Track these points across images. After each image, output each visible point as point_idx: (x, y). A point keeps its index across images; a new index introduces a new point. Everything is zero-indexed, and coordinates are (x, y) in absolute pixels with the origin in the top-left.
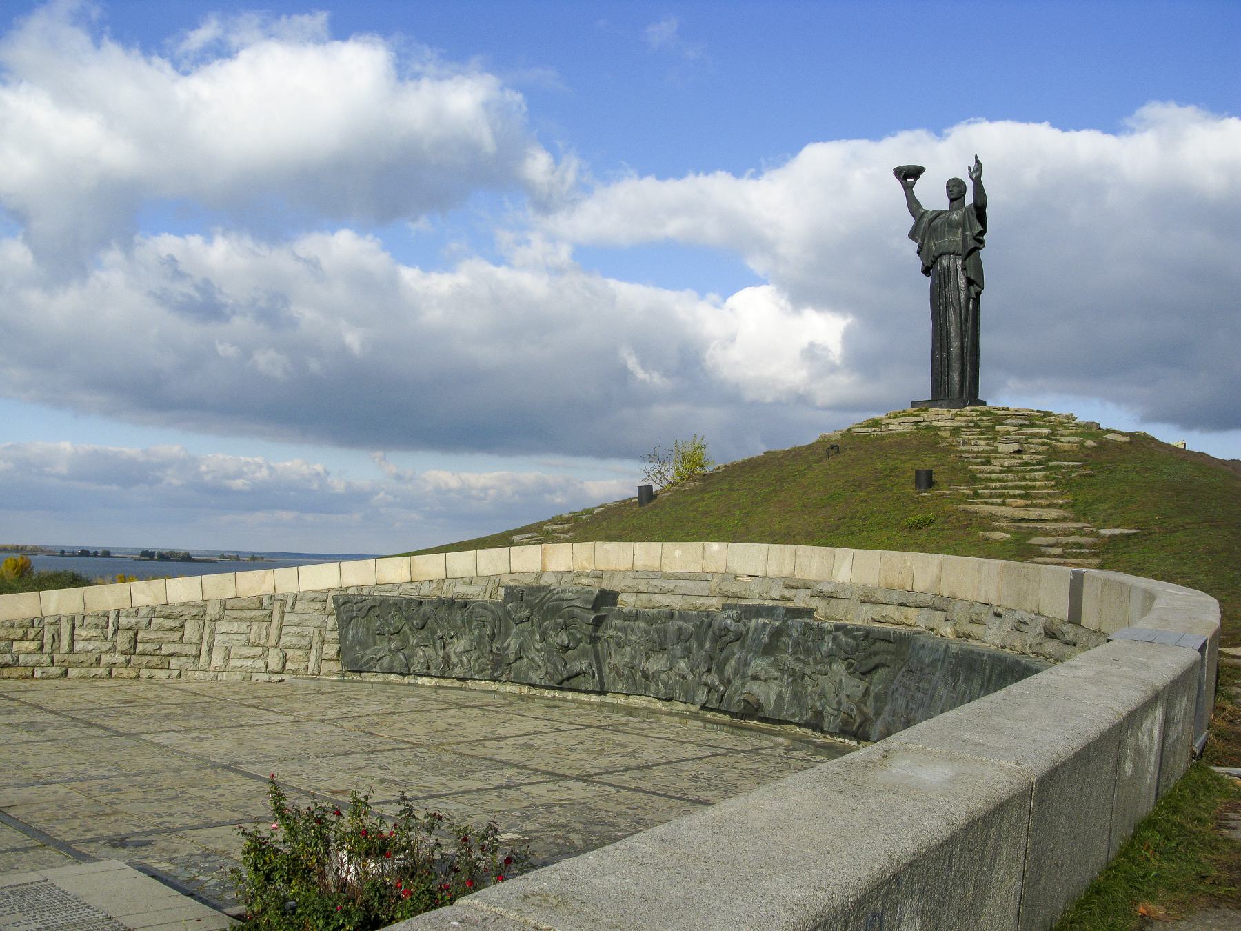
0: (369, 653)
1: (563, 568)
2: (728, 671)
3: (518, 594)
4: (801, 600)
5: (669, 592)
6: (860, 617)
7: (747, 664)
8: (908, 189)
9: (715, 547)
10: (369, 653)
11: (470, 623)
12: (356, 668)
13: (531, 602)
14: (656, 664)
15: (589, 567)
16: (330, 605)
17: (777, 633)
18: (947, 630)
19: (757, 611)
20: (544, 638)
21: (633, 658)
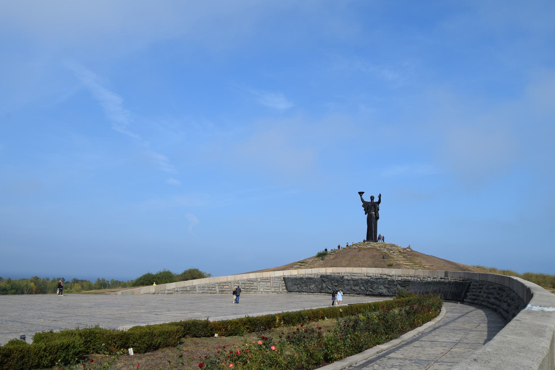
0: (293, 288)
2: (374, 288)
3: (322, 276)
4: (385, 276)
6: (400, 278)
8: (361, 196)
10: (293, 288)
12: (290, 291)
13: (324, 278)
14: (356, 288)
15: (336, 272)
16: (282, 279)
17: (383, 282)
18: (419, 280)
19: (379, 279)
20: (332, 284)
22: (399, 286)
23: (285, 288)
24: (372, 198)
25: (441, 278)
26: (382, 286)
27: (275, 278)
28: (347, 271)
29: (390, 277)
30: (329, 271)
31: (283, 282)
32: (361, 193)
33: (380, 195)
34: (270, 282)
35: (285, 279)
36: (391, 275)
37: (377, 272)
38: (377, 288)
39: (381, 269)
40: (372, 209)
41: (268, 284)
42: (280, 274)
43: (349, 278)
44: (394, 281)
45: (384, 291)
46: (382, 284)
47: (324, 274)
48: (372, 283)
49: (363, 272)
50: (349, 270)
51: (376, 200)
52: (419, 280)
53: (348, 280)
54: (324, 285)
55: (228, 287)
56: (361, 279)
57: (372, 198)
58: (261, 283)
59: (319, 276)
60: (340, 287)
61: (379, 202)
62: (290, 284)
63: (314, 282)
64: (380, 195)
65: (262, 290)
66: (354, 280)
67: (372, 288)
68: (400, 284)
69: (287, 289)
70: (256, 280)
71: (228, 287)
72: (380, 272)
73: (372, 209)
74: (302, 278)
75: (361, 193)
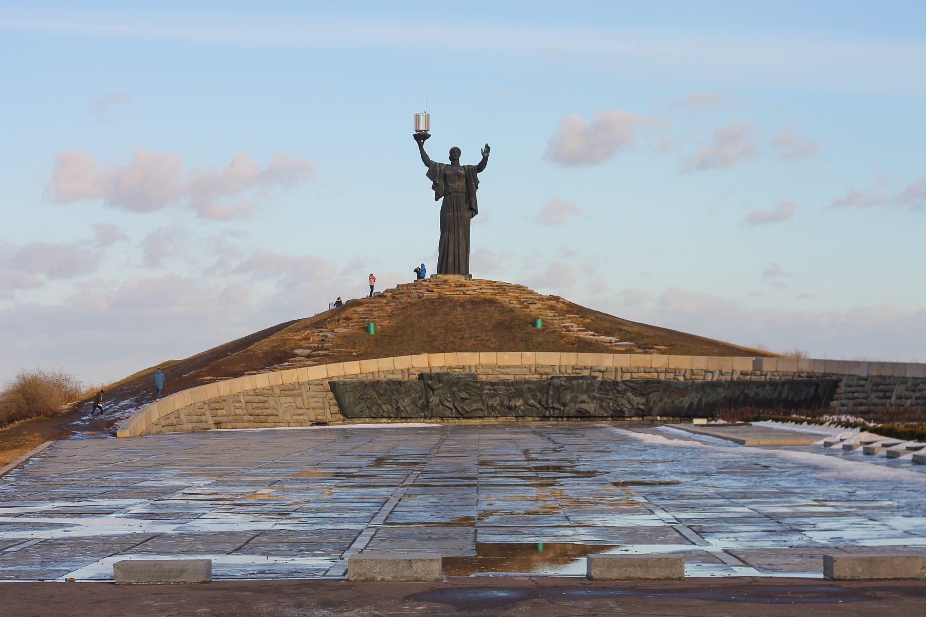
1: (441, 365)
4: (586, 373)
5: (507, 374)
6: (627, 377)
7: (576, 397)
9: (528, 354)
11: (409, 391)
14: (519, 403)
15: (454, 364)
18: (681, 378)
20: (453, 394)
21: (501, 401)
22: (629, 394)
23: (336, 409)
24: (455, 154)
25: (742, 374)
26: (585, 397)
27: (310, 383)
28: (483, 362)
29: (600, 375)
30: (439, 361)
31: (331, 395)
32: (421, 137)
33: (487, 147)
34: (300, 395)
35: (334, 386)
36: (603, 369)
37: (564, 363)
39: (573, 354)
40: (457, 187)
41: (299, 399)
43: (492, 378)
44: (615, 383)
45: (591, 407)
46: (586, 392)
47: (428, 371)
48: (559, 389)
49: (526, 362)
50: (487, 358)
51: (469, 159)
52: (681, 378)
53: (492, 384)
54: (434, 400)
55: (224, 412)
56: (527, 382)
57: (455, 154)
58: (283, 400)
59: (414, 377)
60: (475, 402)
62: (348, 399)
63: (408, 393)
64: (487, 147)
65: (288, 417)
66: (505, 383)
67: (559, 401)
68: (633, 390)
70: (269, 391)
71: (224, 412)
72: (573, 363)
73: (457, 187)
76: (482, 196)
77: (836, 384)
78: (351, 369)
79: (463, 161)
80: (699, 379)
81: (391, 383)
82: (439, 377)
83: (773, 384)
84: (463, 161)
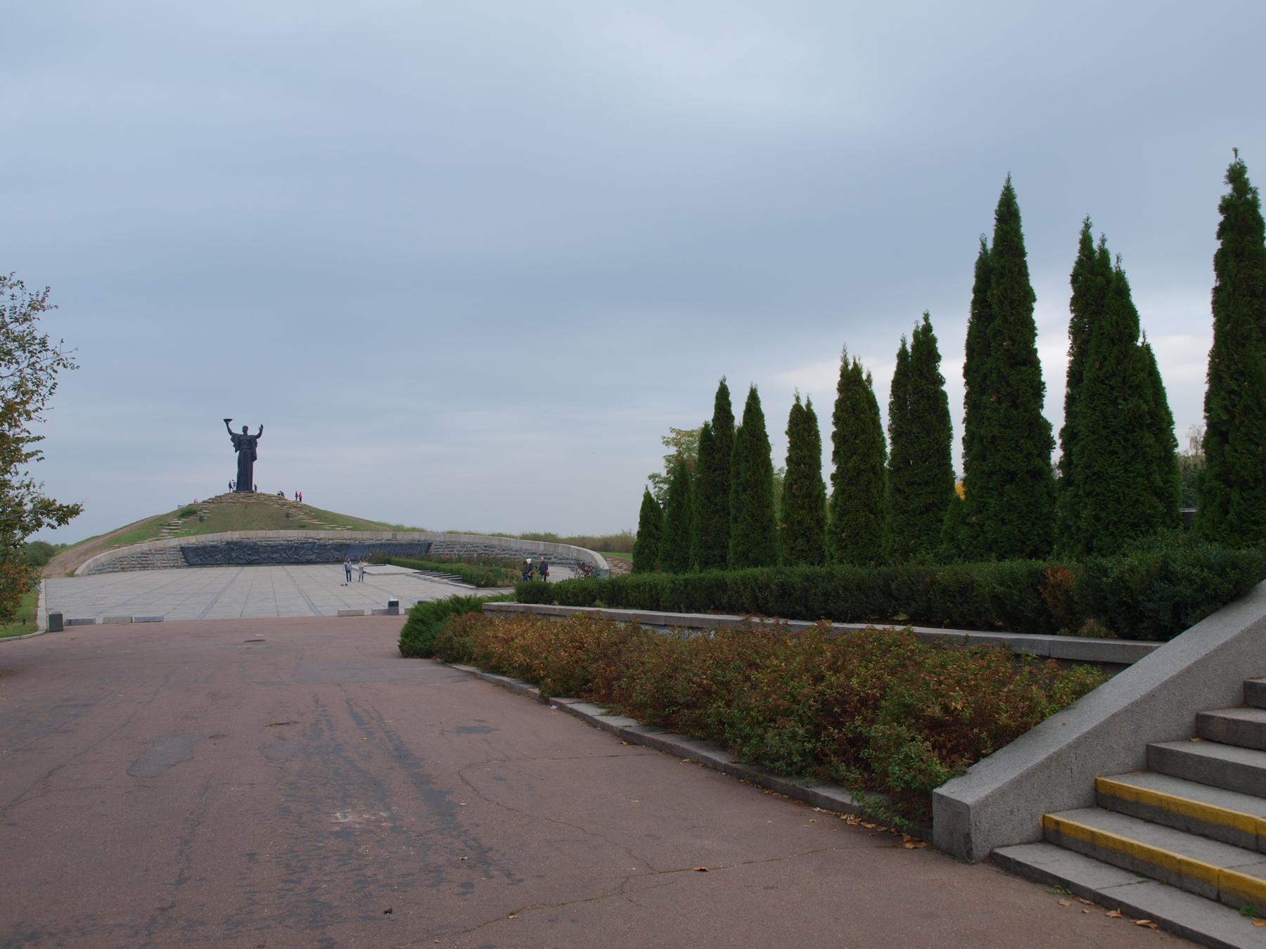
13: (231, 546)
24: (245, 429)
30: (235, 536)
32: (227, 421)
35: (183, 549)
38: (305, 554)
42: (175, 542)
50: (261, 533)
51: (253, 432)
57: (245, 429)
61: (259, 435)
69: (187, 561)
74: (204, 548)
75: (227, 421)
76: (259, 451)
77: (430, 545)
78: (192, 540)
79: (249, 433)
80: (367, 543)
81: (212, 547)
82: (236, 543)
83: (401, 545)
84: (249, 433)
